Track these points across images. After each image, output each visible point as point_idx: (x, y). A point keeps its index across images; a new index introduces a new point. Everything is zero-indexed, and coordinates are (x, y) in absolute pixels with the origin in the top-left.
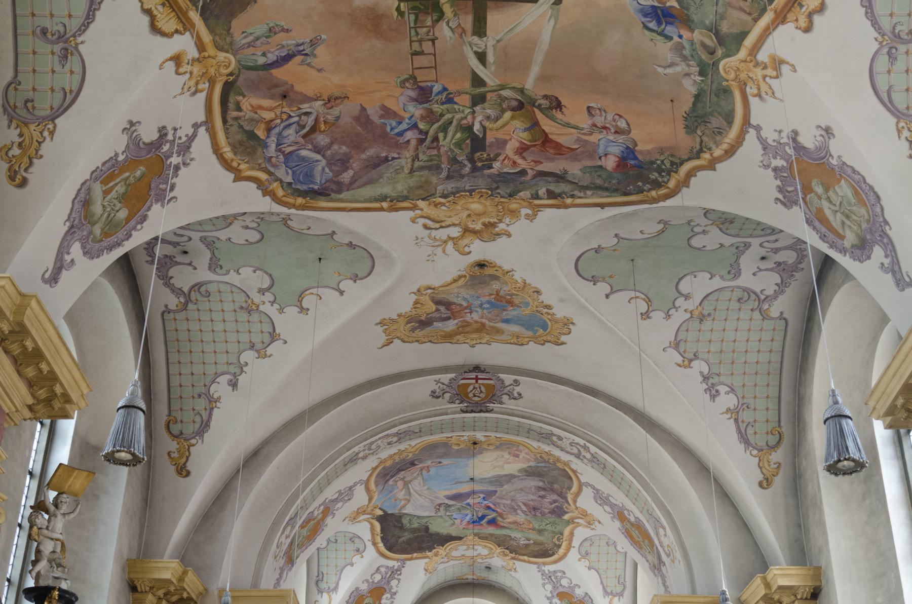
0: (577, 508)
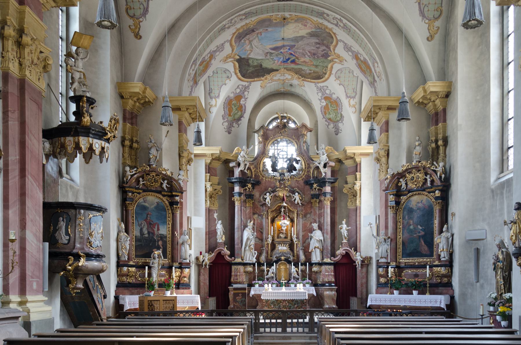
0: (335, 53)
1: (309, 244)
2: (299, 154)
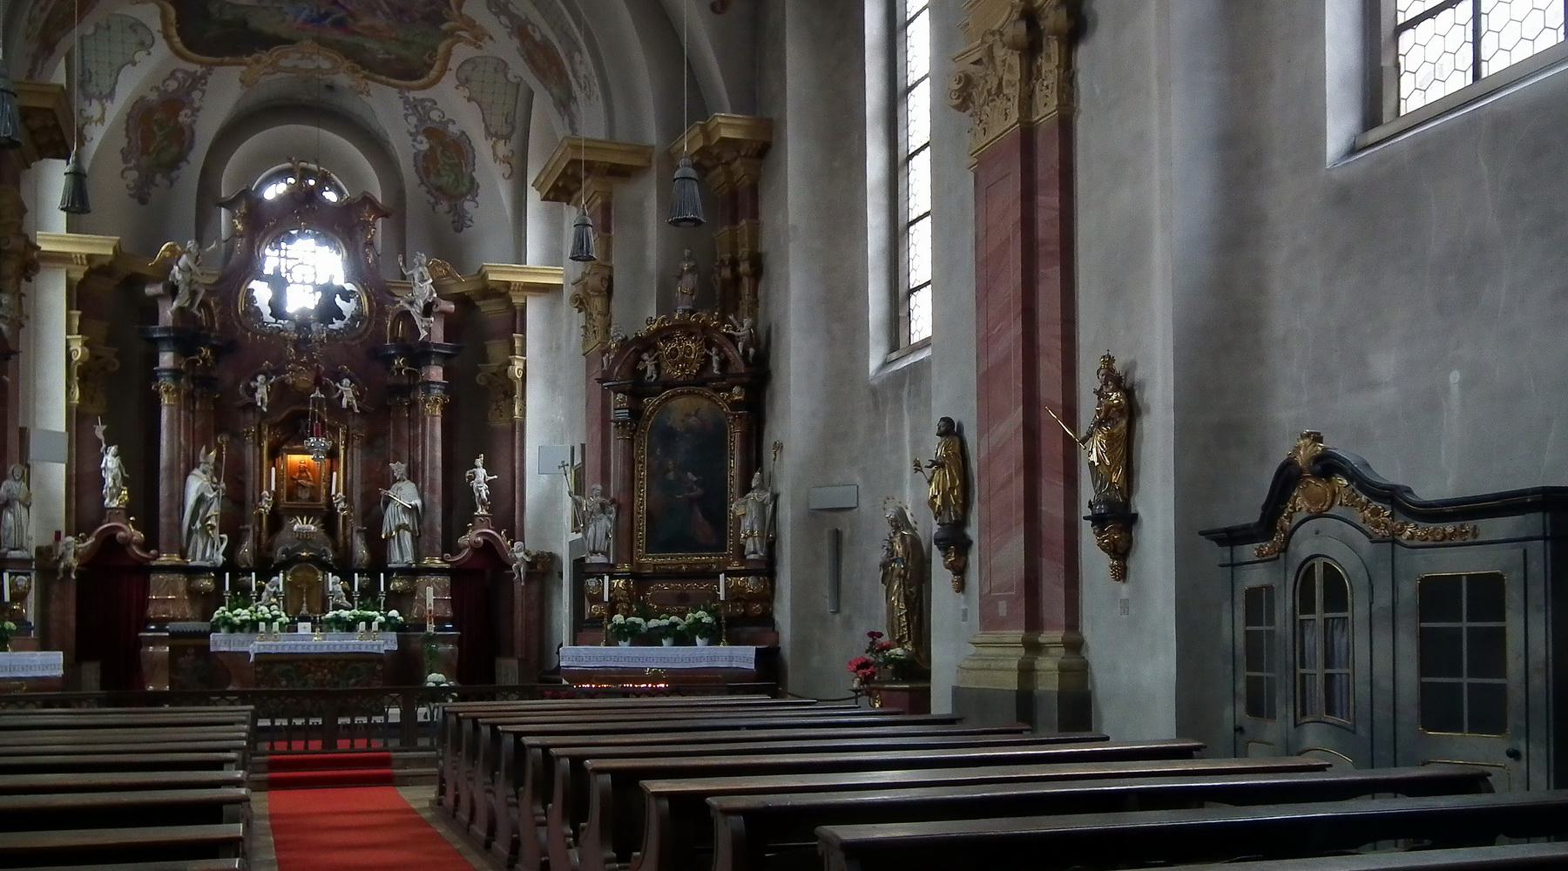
0: (461, 15)
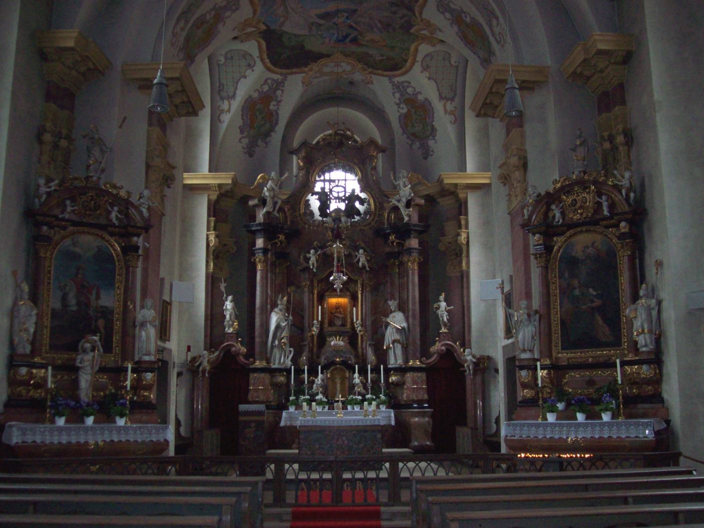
1: (383, 336)
2: (365, 187)
